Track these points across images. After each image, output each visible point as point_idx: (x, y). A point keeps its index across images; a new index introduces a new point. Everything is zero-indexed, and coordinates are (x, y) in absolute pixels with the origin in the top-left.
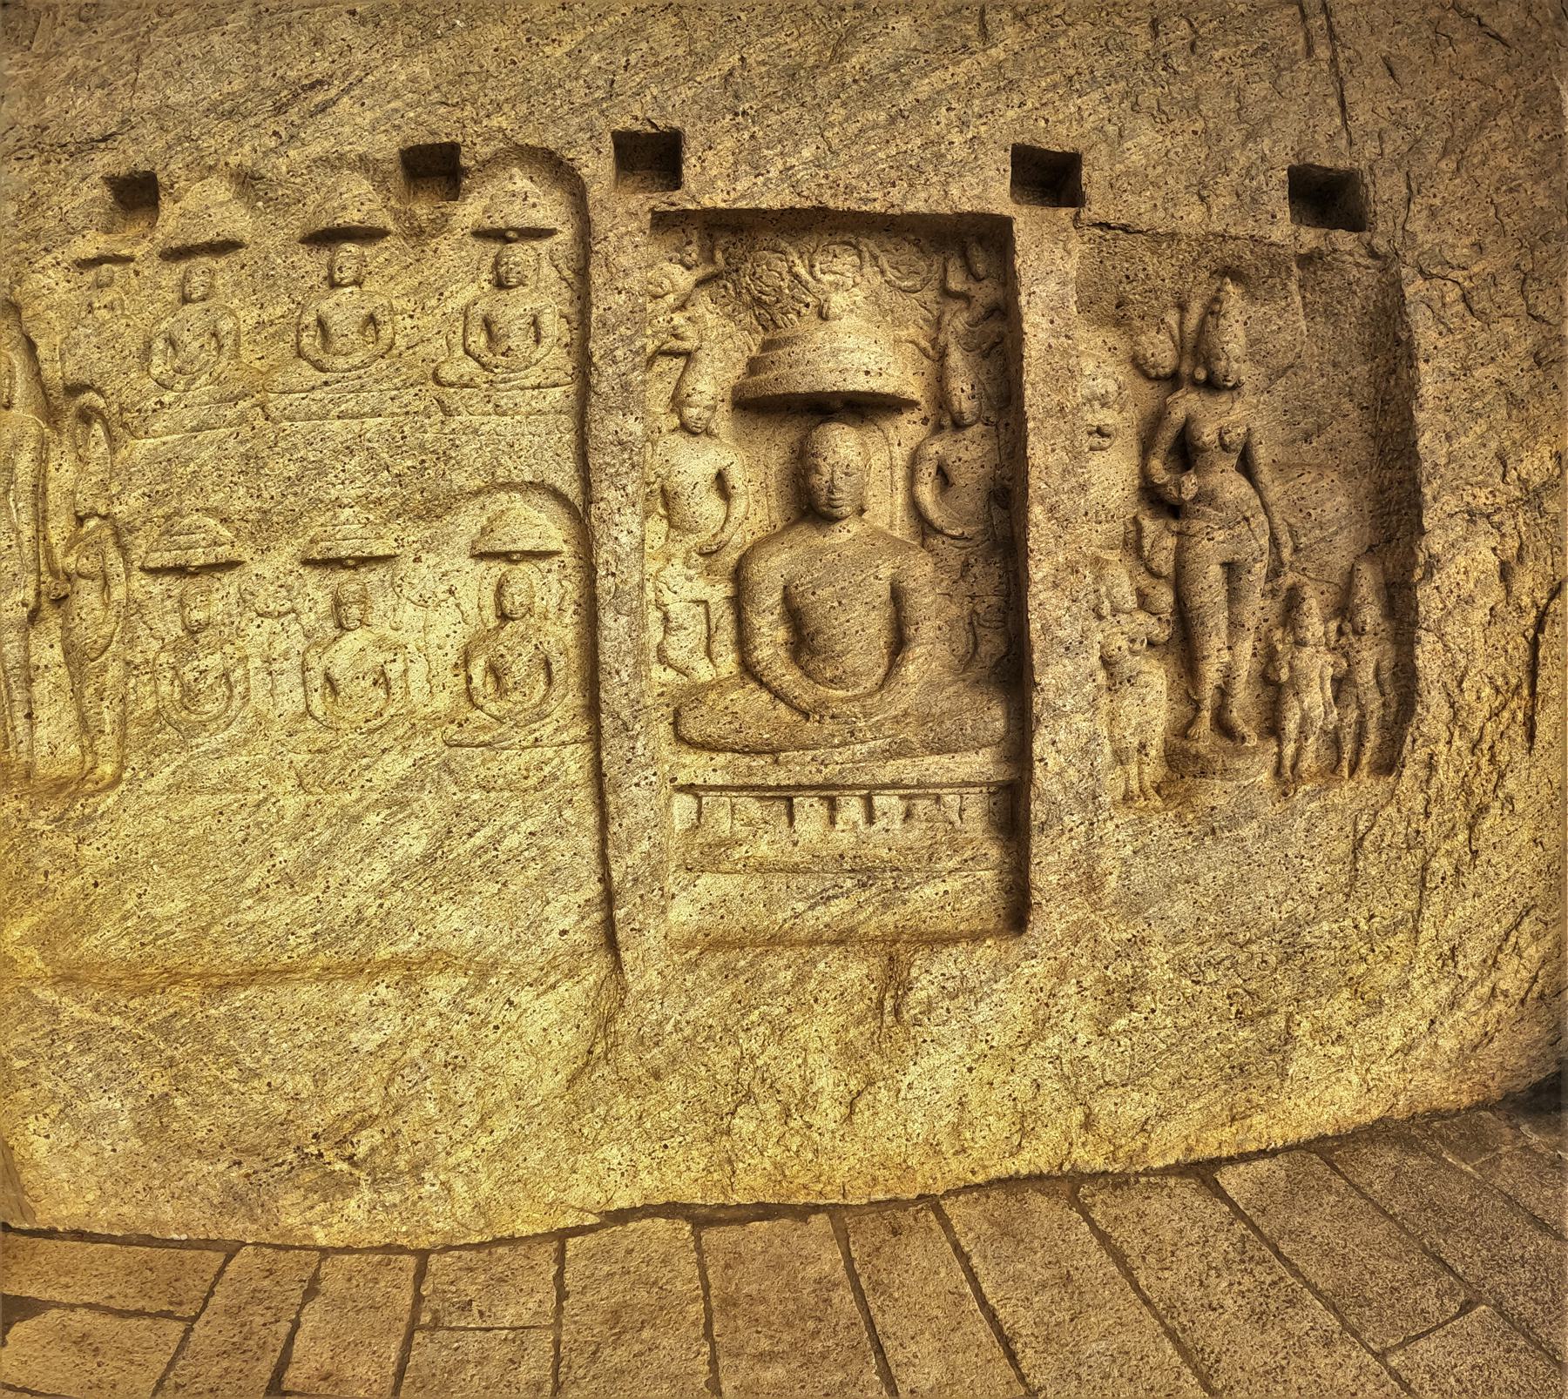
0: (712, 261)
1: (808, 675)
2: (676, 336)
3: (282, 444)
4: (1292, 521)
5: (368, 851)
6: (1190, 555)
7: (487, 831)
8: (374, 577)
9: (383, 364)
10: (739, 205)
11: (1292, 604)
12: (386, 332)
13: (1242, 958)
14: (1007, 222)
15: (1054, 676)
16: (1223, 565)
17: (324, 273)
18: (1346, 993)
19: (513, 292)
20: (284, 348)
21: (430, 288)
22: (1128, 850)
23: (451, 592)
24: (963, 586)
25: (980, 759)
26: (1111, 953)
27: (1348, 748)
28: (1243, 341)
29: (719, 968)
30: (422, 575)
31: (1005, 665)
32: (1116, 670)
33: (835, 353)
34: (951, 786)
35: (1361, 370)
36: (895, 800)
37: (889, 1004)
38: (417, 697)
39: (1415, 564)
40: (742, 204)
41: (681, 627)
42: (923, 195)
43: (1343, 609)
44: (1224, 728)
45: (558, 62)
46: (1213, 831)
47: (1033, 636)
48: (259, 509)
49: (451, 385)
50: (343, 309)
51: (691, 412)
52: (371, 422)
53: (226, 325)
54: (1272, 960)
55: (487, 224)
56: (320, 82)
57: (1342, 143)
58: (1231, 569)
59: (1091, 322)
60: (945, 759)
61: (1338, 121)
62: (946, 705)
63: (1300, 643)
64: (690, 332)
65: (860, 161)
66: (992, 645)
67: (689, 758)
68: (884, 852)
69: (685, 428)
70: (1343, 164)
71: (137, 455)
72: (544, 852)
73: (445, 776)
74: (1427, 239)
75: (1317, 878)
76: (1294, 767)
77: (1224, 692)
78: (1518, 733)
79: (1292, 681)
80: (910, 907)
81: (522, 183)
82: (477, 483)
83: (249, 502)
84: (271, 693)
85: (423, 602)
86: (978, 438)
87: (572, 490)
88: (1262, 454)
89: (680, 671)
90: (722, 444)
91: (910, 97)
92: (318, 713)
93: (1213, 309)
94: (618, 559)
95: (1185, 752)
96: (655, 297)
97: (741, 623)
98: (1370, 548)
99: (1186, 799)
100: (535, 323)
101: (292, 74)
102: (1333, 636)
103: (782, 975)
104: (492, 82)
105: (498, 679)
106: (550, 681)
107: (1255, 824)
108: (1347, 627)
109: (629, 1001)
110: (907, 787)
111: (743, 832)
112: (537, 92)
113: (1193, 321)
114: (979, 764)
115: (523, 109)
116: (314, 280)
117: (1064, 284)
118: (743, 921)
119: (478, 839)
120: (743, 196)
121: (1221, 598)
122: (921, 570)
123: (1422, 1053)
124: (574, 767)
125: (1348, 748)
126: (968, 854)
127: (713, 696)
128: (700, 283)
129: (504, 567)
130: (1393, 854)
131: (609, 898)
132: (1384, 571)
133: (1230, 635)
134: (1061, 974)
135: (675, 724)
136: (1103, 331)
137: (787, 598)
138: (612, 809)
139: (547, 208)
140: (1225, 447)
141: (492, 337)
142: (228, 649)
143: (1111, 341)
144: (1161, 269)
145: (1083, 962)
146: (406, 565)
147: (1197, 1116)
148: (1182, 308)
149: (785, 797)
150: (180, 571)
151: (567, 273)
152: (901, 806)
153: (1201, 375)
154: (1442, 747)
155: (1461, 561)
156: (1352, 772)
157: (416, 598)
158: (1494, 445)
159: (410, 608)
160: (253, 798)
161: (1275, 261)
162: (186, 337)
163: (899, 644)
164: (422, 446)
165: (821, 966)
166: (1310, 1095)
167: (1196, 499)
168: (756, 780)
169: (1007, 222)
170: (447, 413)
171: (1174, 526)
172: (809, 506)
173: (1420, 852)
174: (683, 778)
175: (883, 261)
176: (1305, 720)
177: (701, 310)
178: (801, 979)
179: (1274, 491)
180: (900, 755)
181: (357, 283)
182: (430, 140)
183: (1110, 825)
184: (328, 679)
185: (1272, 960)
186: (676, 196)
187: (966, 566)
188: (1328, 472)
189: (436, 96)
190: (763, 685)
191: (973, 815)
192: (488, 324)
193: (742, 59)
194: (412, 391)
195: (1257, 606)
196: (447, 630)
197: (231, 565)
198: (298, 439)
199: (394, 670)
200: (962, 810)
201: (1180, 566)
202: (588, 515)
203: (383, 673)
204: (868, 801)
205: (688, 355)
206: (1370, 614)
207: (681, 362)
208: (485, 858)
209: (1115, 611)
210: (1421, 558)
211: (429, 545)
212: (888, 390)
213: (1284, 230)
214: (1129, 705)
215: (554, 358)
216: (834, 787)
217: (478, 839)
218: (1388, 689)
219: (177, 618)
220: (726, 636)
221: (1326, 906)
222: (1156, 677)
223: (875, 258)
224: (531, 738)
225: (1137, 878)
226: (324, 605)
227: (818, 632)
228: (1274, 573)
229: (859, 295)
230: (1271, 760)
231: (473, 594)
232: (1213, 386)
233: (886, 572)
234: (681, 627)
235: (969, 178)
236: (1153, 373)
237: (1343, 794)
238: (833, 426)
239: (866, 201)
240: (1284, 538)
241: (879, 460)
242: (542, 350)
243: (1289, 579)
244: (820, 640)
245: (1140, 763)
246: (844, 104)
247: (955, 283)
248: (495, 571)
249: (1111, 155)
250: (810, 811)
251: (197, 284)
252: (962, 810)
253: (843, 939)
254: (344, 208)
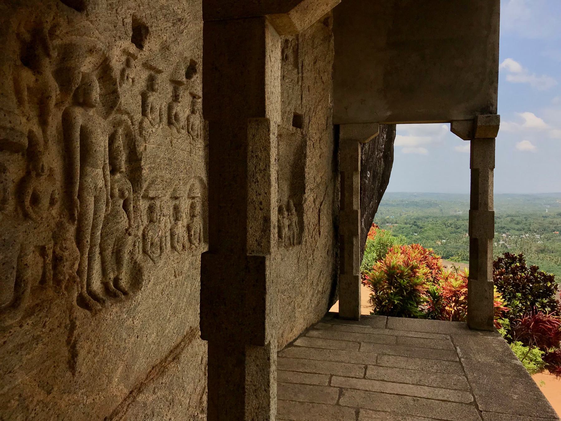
27: (292, 240)
35: (292, 158)
63: (283, 218)
108: (290, 214)
125: (292, 240)
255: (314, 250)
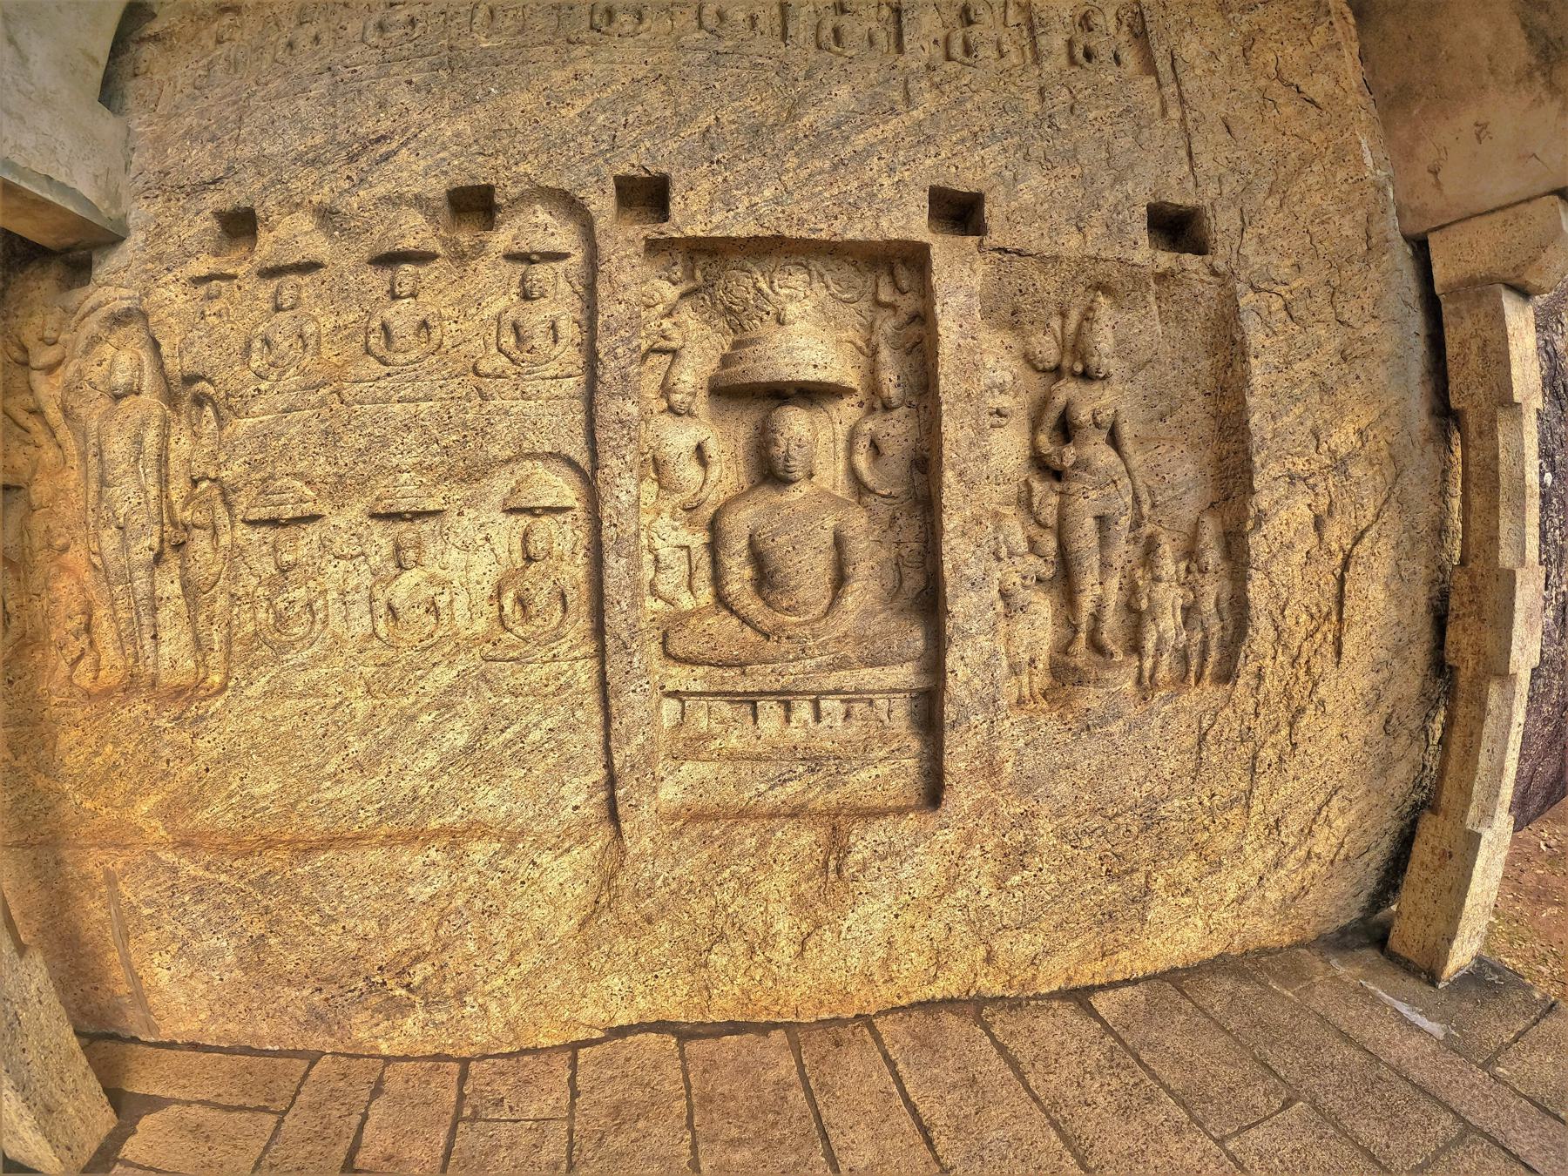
0: (693, 278)
1: (769, 605)
2: (664, 337)
3: (354, 423)
4: (1150, 483)
5: (422, 744)
6: (1070, 510)
7: (516, 728)
8: (426, 527)
9: (434, 359)
10: (714, 234)
11: (1150, 549)
12: (436, 334)
13: (1111, 828)
14: (924, 248)
15: (962, 605)
16: (1096, 518)
17: (387, 287)
18: (1193, 856)
19: (536, 303)
20: (356, 347)
21: (470, 300)
22: (1021, 743)
23: (487, 539)
24: (891, 534)
25: (904, 671)
26: (1007, 824)
27: (1194, 662)
28: (1111, 341)
29: (699, 836)
30: (465, 525)
31: (927, 600)
32: (1012, 601)
33: (790, 351)
34: (881, 692)
35: (1205, 364)
36: (837, 703)
37: (832, 864)
38: (461, 622)
39: (1247, 517)
40: (717, 234)
41: (668, 567)
42: (860, 226)
43: (1191, 553)
44: (1096, 646)
45: (572, 121)
46: (1088, 728)
47: (946, 574)
48: (335, 474)
49: (487, 376)
50: (401, 315)
51: (676, 398)
52: (424, 405)
53: (310, 329)
54: (1135, 830)
55: (515, 249)
56: (384, 137)
57: (1190, 185)
58: (1101, 520)
59: (991, 326)
60: (876, 671)
61: (1186, 168)
62: (877, 628)
63: (1157, 580)
64: (675, 334)
65: (809, 199)
66: (914, 581)
67: (675, 670)
68: (828, 745)
69: (671, 409)
70: (1190, 202)
71: (240, 432)
72: (561, 744)
73: (483, 685)
74: (1256, 261)
75: (1170, 764)
76: (1152, 677)
77: (1096, 618)
78: (1328, 650)
79: (1151, 609)
80: (849, 788)
81: (543, 216)
82: (508, 453)
83: (328, 468)
84: (345, 619)
85: (465, 548)
86: (902, 418)
87: (583, 459)
88: (1126, 431)
89: (669, 602)
90: (701, 423)
91: (849, 149)
92: (382, 635)
93: (1088, 317)
94: (619, 513)
95: (1066, 666)
96: (648, 307)
97: (715, 563)
98: (1212, 505)
99: (1067, 703)
100: (553, 327)
101: (363, 130)
102: (1182, 574)
103: (748, 841)
104: (519, 137)
105: (524, 608)
106: (565, 610)
107: (1121, 722)
108: (1194, 567)
109: (627, 862)
110: (847, 693)
111: (718, 729)
112: (555, 145)
113: (1072, 325)
114: (903, 675)
115: (544, 158)
116: (380, 293)
117: (970, 296)
118: (718, 799)
119: (508, 735)
120: (717, 227)
121: (1094, 544)
122: (857, 522)
123: (1252, 902)
124: (584, 678)
125: (1194, 662)
126: (895, 746)
127: (694, 621)
128: (683, 296)
129: (529, 519)
130: (1230, 746)
131: (612, 781)
132: (1223, 522)
133: (1101, 573)
134: (968, 841)
135: (664, 643)
136: (1001, 334)
137: (752, 544)
138: (614, 710)
139: (563, 237)
140: (1097, 425)
141: (519, 339)
142: (311, 584)
143: (1008, 341)
144: (1047, 284)
145: (986, 831)
146: (452, 518)
147: (1076, 952)
148: (1064, 315)
149: (751, 701)
150: (274, 522)
151: (579, 288)
152: (842, 708)
153: (1079, 368)
154: (1268, 661)
155: (1283, 514)
156: (1198, 681)
157: (459, 544)
158: (1309, 423)
159: (454, 552)
160: (331, 702)
161: (1136, 278)
162: (279, 338)
163: (840, 580)
164: (464, 424)
165: (779, 834)
166: (1164, 936)
167: (1075, 466)
168: (728, 688)
169: (924, 248)
170: (484, 398)
171: (1058, 487)
172: (770, 471)
173: (1251, 745)
174: (670, 687)
175: (828, 278)
176: (1161, 640)
177: (684, 317)
178: (763, 845)
179: (1136, 460)
180: (841, 668)
181: (413, 295)
182: (470, 183)
183: (1007, 723)
184: (391, 608)
185: (1135, 830)
186: (665, 227)
187: (894, 519)
188: (1178, 444)
189: (475, 148)
190: (732, 612)
191: (899, 716)
192: (516, 328)
193: (717, 119)
194: (456, 381)
195: (1123, 550)
196: (483, 569)
197: (314, 518)
198: (366, 419)
199: (442, 601)
200: (890, 711)
201: (1062, 518)
202: (595, 478)
203: (434, 604)
204: (816, 705)
205: (674, 352)
206: (1212, 557)
207: (669, 358)
208: (514, 749)
209: (1011, 554)
210: (1252, 513)
211: (469, 502)
212: (832, 380)
213: (1145, 253)
214: (1021, 628)
215: (568, 354)
216: (789, 693)
217: (508, 735)
218: (1225, 616)
219: (271, 560)
220: (704, 574)
221: (1177, 787)
222: (1043, 607)
223: (822, 276)
224: (550, 654)
225: (1028, 765)
226: (387, 549)
227: (776, 571)
228: (1136, 524)
229: (809, 305)
230: (1134, 672)
231: (505, 541)
232: (1087, 376)
233: (830, 523)
234: (668, 567)
235: (896, 213)
236: (1041, 366)
237: (1189, 698)
238: (789, 408)
239: (814, 231)
240: (1144, 496)
241: (824, 435)
242: (559, 349)
243: (1148, 529)
244: (778, 577)
245: (1031, 674)
246: (797, 155)
247: (885, 295)
248: (521, 522)
249: (1007, 194)
250: (771, 713)
251: (287, 297)
252: (890, 711)
253: (796, 813)
254: (403, 236)
255: (1301, 711)
